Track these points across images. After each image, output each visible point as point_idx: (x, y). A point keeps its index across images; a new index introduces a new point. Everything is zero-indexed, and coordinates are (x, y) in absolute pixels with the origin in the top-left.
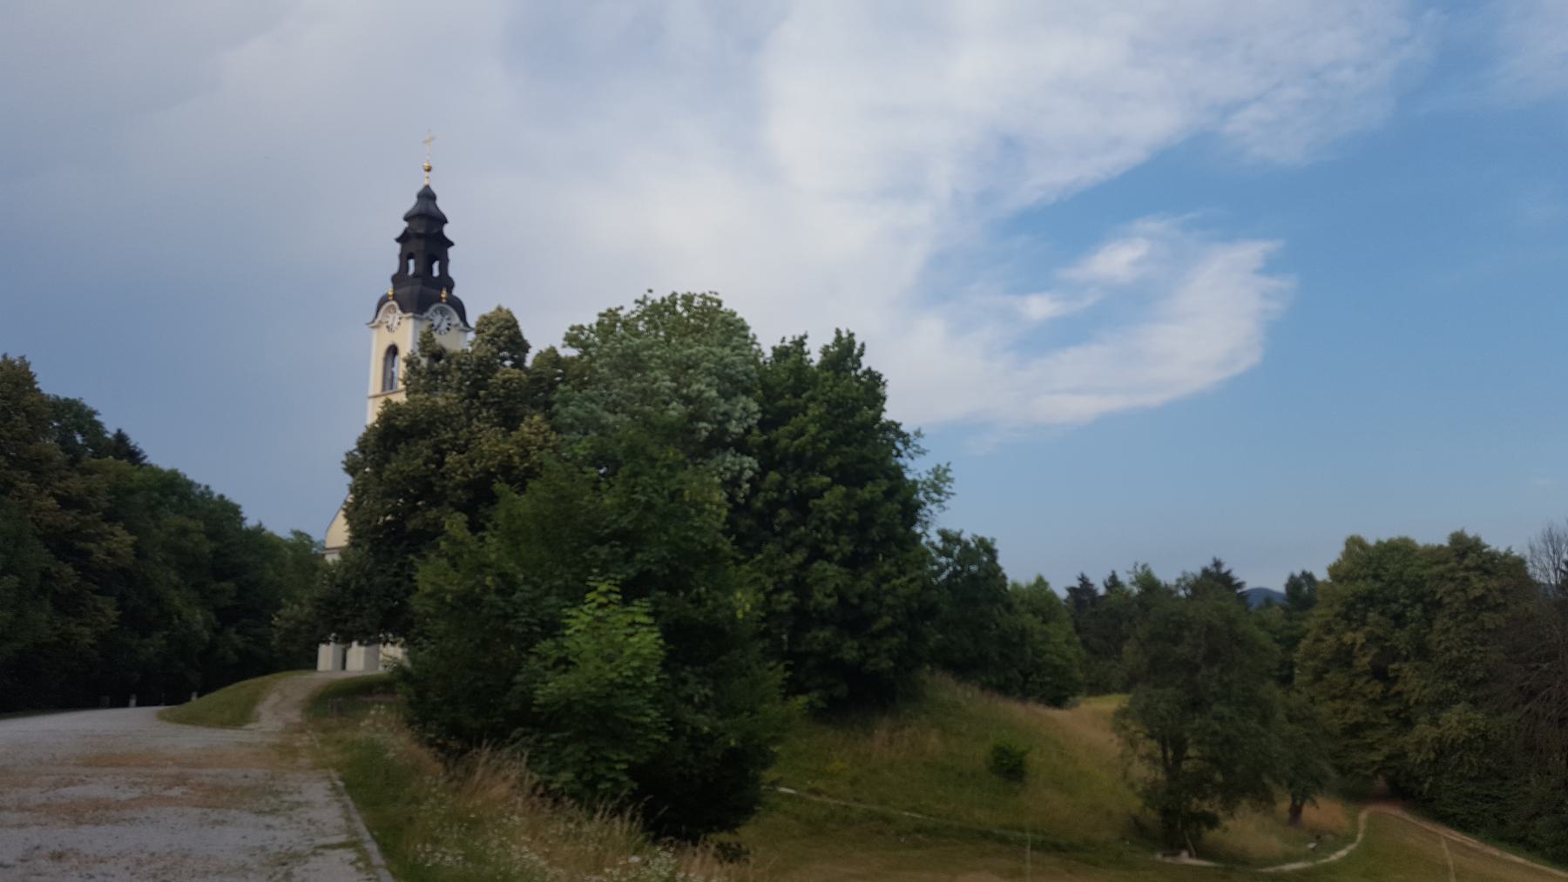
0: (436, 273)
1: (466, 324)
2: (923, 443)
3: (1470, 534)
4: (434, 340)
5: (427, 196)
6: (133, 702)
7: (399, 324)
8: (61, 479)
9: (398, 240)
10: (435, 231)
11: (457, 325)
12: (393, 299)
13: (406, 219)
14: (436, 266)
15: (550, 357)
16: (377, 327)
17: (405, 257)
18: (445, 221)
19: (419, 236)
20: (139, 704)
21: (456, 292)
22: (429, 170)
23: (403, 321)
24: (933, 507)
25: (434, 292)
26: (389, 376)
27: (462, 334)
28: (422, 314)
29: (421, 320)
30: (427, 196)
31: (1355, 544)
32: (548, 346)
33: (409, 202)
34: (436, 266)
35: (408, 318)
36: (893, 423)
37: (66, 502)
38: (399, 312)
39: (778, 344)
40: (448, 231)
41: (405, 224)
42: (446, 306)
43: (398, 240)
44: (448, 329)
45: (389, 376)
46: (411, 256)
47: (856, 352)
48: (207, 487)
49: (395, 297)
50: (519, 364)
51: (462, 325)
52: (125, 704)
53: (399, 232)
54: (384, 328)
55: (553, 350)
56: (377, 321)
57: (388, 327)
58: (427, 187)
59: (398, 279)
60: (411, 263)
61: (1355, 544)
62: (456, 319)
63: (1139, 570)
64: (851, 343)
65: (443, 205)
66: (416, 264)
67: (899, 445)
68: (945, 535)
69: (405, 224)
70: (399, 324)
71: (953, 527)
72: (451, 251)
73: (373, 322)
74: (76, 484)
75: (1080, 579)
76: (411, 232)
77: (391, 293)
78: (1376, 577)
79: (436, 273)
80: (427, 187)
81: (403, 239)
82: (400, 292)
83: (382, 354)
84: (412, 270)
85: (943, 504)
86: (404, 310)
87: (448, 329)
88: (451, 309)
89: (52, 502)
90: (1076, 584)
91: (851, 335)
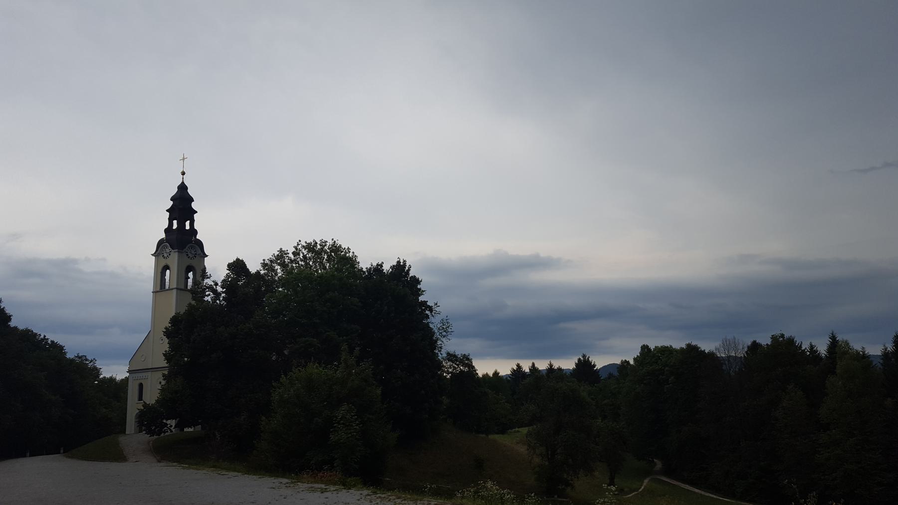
0: (188, 227)
2: (438, 309)
3: (694, 343)
5: (183, 188)
7: (170, 255)
9: (167, 211)
11: (199, 254)
13: (171, 200)
14: (188, 223)
17: (170, 221)
21: (198, 237)
22: (183, 173)
23: (172, 253)
24: (444, 340)
28: (183, 250)
29: (182, 252)
30: (183, 188)
32: (256, 271)
33: (175, 191)
34: (188, 223)
36: (425, 301)
38: (170, 248)
39: (369, 266)
40: (194, 205)
41: (172, 202)
43: (167, 211)
44: (195, 257)
47: (407, 269)
48: (45, 336)
51: (202, 254)
53: (169, 207)
56: (157, 252)
57: (163, 256)
58: (183, 183)
59: (166, 231)
60: (175, 222)
61: (645, 348)
62: (200, 251)
66: (178, 224)
67: (427, 312)
68: (448, 354)
71: (451, 351)
72: (195, 215)
73: (155, 253)
79: (188, 227)
80: (183, 183)
84: (175, 226)
88: (197, 246)
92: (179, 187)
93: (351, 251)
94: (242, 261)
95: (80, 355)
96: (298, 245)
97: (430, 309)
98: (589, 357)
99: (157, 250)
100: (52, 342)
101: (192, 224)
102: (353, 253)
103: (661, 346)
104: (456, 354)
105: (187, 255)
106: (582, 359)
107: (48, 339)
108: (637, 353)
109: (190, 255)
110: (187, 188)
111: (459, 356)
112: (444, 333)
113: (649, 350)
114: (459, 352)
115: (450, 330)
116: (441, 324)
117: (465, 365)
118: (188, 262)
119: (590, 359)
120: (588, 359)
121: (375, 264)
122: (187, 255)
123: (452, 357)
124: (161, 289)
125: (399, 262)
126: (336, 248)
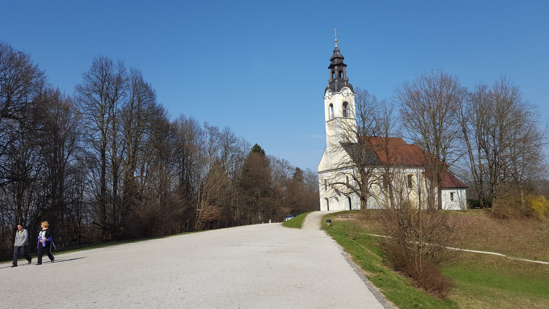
0: (342, 77)
6: (270, 222)
7: (332, 96)
9: (329, 68)
10: (340, 62)
11: (351, 93)
13: (331, 60)
16: (325, 99)
18: (344, 58)
19: (336, 65)
20: (272, 222)
21: (349, 82)
25: (343, 83)
28: (339, 92)
29: (339, 94)
33: (331, 55)
34: (342, 74)
40: (344, 62)
41: (331, 62)
43: (329, 68)
44: (348, 95)
51: (352, 93)
52: (268, 222)
56: (325, 97)
62: (351, 92)
65: (343, 53)
77: (329, 86)
81: (332, 67)
82: (330, 85)
92: (334, 52)
105: (343, 95)
109: (345, 95)
110: (339, 51)
122: (343, 95)
124: (329, 118)
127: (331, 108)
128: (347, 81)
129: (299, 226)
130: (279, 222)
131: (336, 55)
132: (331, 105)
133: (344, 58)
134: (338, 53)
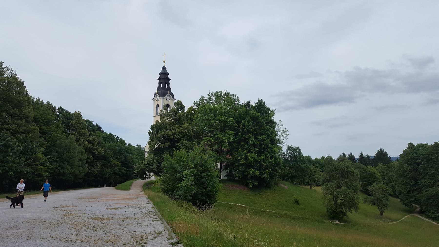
0: (167, 87)
1: (174, 99)
4: (161, 118)
5: (164, 68)
6: (105, 186)
7: (159, 99)
8: (88, 137)
9: (158, 79)
11: (172, 99)
12: (157, 94)
13: (160, 74)
15: (191, 109)
17: (160, 84)
19: (163, 78)
20: (106, 187)
22: (164, 62)
23: (160, 99)
25: (167, 91)
26: (157, 112)
27: (173, 101)
29: (164, 98)
30: (164, 68)
31: (410, 145)
33: (160, 70)
35: (161, 98)
37: (90, 142)
39: (243, 103)
40: (169, 77)
41: (160, 76)
42: (169, 95)
43: (158, 79)
44: (170, 100)
45: (157, 112)
46: (161, 83)
48: (117, 136)
49: (158, 93)
50: (183, 112)
51: (173, 99)
52: (104, 187)
54: (156, 100)
55: (192, 107)
58: (164, 66)
59: (158, 89)
60: (161, 84)
61: (410, 145)
62: (172, 98)
63: (328, 156)
64: (262, 101)
68: (288, 146)
69: (160, 76)
70: (159, 99)
73: (153, 99)
74: (91, 138)
75: (343, 154)
76: (161, 77)
78: (416, 153)
80: (164, 66)
81: (159, 79)
83: (155, 107)
84: (161, 87)
85: (287, 137)
86: (160, 97)
87: (170, 100)
88: (171, 95)
89: (87, 142)
90: (342, 155)
91: (261, 99)
93: (237, 96)
94: (180, 101)
95: (138, 145)
96: (210, 93)
97: (275, 123)
98: (384, 150)
99: (154, 98)
100: (121, 139)
101: (169, 86)
102: (238, 96)
103: (420, 144)
104: (293, 146)
105: (166, 99)
106: (380, 151)
107: (119, 137)
108: (405, 147)
109: (167, 99)
110: (166, 69)
111: (294, 148)
112: (285, 136)
113: (413, 146)
114: (294, 146)
115: (287, 134)
116: (283, 131)
117: (296, 152)
118: (167, 103)
119: (384, 151)
120: (383, 151)
121: (246, 101)
122: (166, 99)
123: (290, 148)
125: (259, 100)
126: (228, 94)
127: (157, 108)
128: (170, 91)
129: (127, 189)
130: (112, 187)
131: (163, 71)
132: (158, 106)
133: (169, 74)
134: (165, 70)
